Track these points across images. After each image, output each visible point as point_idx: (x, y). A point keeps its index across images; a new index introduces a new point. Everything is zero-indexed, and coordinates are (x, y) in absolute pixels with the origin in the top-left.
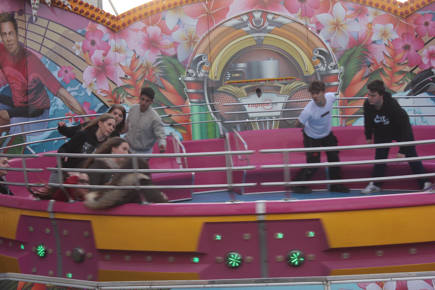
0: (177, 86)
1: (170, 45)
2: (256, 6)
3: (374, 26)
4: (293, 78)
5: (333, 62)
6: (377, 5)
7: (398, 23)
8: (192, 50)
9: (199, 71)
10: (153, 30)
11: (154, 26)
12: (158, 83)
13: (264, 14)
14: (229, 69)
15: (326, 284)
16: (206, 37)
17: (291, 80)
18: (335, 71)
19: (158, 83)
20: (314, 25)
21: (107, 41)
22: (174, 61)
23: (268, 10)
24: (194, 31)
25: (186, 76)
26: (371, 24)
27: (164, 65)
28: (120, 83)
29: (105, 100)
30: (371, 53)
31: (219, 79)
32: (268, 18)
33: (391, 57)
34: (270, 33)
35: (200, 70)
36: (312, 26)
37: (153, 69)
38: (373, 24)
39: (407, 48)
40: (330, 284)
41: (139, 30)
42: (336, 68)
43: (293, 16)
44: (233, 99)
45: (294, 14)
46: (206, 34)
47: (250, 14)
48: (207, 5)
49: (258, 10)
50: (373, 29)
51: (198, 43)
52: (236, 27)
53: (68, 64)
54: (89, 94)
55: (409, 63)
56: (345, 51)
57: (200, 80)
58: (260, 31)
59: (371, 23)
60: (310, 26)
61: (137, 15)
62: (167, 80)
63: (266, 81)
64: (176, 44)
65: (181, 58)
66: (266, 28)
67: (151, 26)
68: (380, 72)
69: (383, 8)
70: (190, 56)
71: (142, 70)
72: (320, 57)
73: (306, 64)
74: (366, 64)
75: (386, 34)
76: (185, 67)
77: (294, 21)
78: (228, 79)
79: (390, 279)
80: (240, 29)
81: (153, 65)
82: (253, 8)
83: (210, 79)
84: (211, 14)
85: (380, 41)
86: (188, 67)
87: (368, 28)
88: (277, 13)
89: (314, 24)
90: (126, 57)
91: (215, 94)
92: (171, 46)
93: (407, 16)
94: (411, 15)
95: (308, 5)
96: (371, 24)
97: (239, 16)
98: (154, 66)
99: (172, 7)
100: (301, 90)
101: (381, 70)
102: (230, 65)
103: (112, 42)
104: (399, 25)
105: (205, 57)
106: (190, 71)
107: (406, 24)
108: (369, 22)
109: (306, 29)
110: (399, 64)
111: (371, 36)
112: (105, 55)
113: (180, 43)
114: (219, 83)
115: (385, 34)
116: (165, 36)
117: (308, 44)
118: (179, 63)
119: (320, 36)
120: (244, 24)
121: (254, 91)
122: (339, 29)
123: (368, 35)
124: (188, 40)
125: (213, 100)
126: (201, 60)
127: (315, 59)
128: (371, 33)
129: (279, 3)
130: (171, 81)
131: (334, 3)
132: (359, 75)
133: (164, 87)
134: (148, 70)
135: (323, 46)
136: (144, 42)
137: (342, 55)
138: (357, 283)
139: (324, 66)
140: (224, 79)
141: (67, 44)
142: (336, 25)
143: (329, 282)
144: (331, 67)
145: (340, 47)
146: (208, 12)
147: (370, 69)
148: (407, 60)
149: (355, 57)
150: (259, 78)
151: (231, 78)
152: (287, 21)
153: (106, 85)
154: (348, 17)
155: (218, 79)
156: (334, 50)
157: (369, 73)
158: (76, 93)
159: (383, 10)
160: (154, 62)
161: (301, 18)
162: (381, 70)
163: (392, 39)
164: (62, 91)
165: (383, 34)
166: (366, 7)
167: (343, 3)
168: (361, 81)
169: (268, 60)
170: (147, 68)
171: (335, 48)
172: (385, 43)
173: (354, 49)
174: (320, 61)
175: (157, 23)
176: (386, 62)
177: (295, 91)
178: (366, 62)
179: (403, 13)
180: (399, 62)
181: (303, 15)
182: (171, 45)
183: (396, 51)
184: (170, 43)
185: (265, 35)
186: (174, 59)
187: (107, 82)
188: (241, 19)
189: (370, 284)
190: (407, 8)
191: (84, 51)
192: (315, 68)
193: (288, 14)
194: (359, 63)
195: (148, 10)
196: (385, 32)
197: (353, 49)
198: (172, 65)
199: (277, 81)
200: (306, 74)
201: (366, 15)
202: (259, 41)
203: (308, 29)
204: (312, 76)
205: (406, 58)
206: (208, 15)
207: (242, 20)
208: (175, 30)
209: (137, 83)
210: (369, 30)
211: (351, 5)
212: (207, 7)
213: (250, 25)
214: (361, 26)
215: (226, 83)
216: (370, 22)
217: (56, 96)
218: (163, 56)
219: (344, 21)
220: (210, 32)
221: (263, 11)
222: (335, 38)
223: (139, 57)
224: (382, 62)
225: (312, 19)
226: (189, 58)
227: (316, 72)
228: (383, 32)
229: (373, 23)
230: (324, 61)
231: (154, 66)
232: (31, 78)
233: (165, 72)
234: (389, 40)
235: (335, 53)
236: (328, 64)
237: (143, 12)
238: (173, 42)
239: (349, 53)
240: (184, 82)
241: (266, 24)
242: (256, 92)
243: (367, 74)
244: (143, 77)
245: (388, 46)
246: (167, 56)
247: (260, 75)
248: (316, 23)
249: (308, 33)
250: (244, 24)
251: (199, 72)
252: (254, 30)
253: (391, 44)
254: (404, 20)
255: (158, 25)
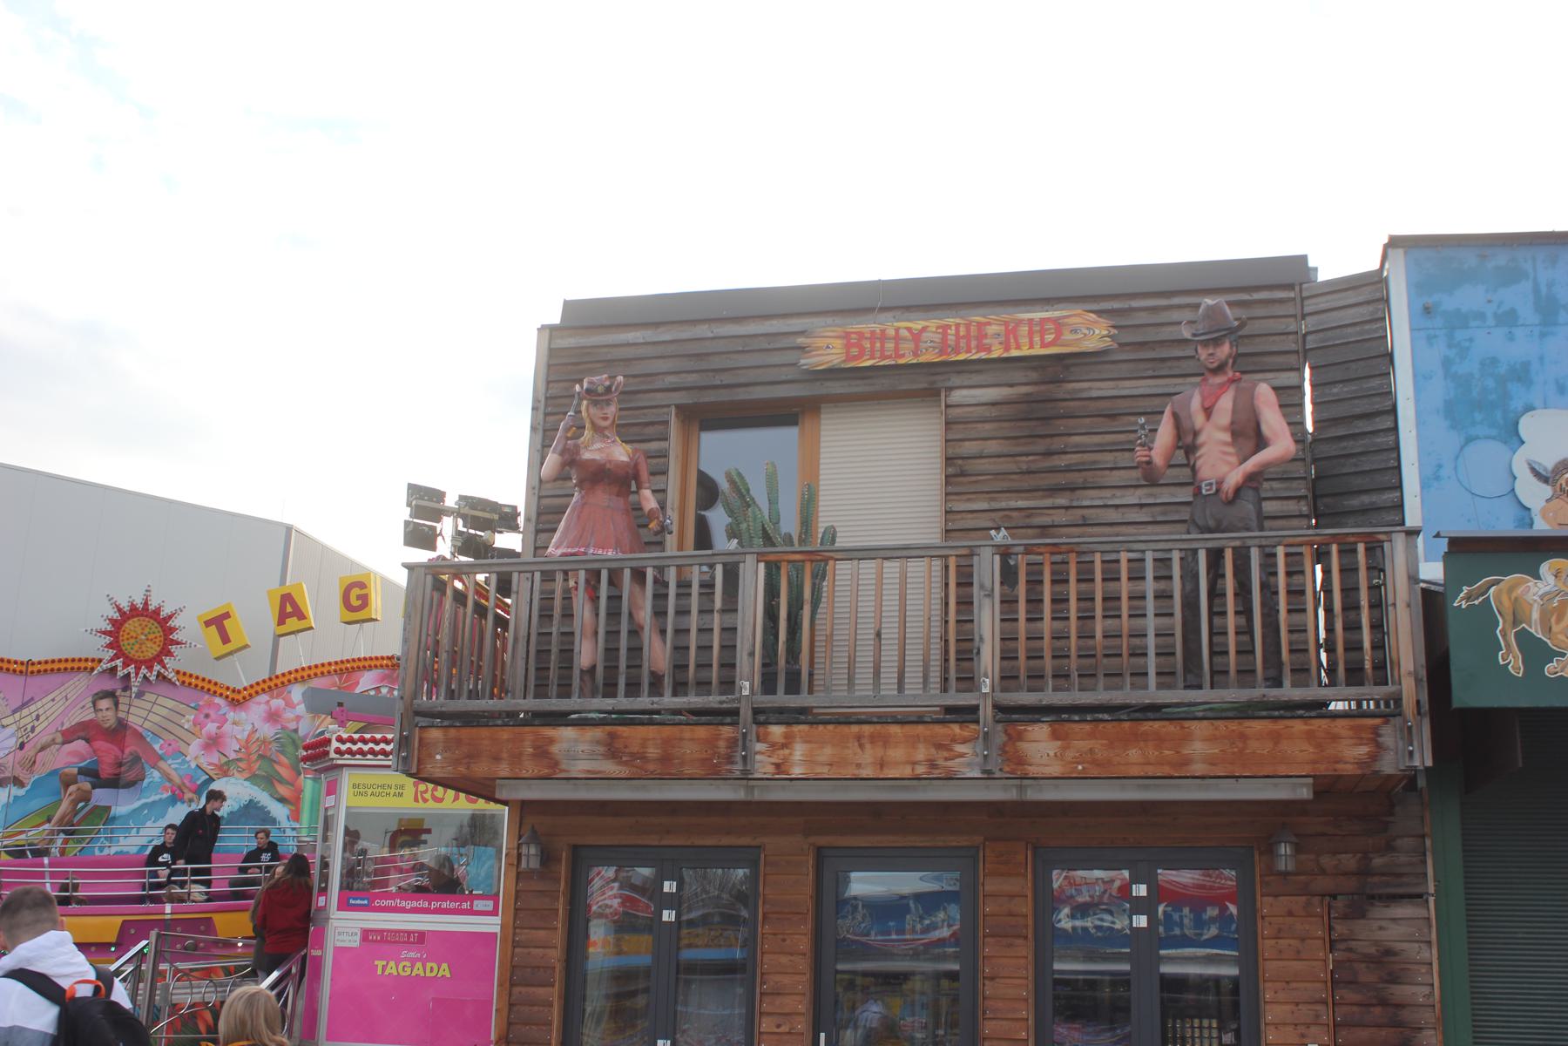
21: (225, 714)
22: (293, 735)
28: (233, 756)
29: (211, 773)
37: (270, 743)
47: (377, 689)
53: (172, 737)
54: (193, 765)
64: (298, 718)
65: (301, 733)
67: (275, 700)
90: (243, 730)
103: (231, 715)
112: (219, 728)
116: (288, 709)
118: (299, 737)
141: (176, 718)
153: (215, 758)
158: (177, 766)
164: (161, 764)
170: (264, 742)
187: (217, 755)
191: (195, 723)
208: (298, 704)
217: (153, 768)
232: (127, 751)
233: (282, 746)
255: (283, 699)
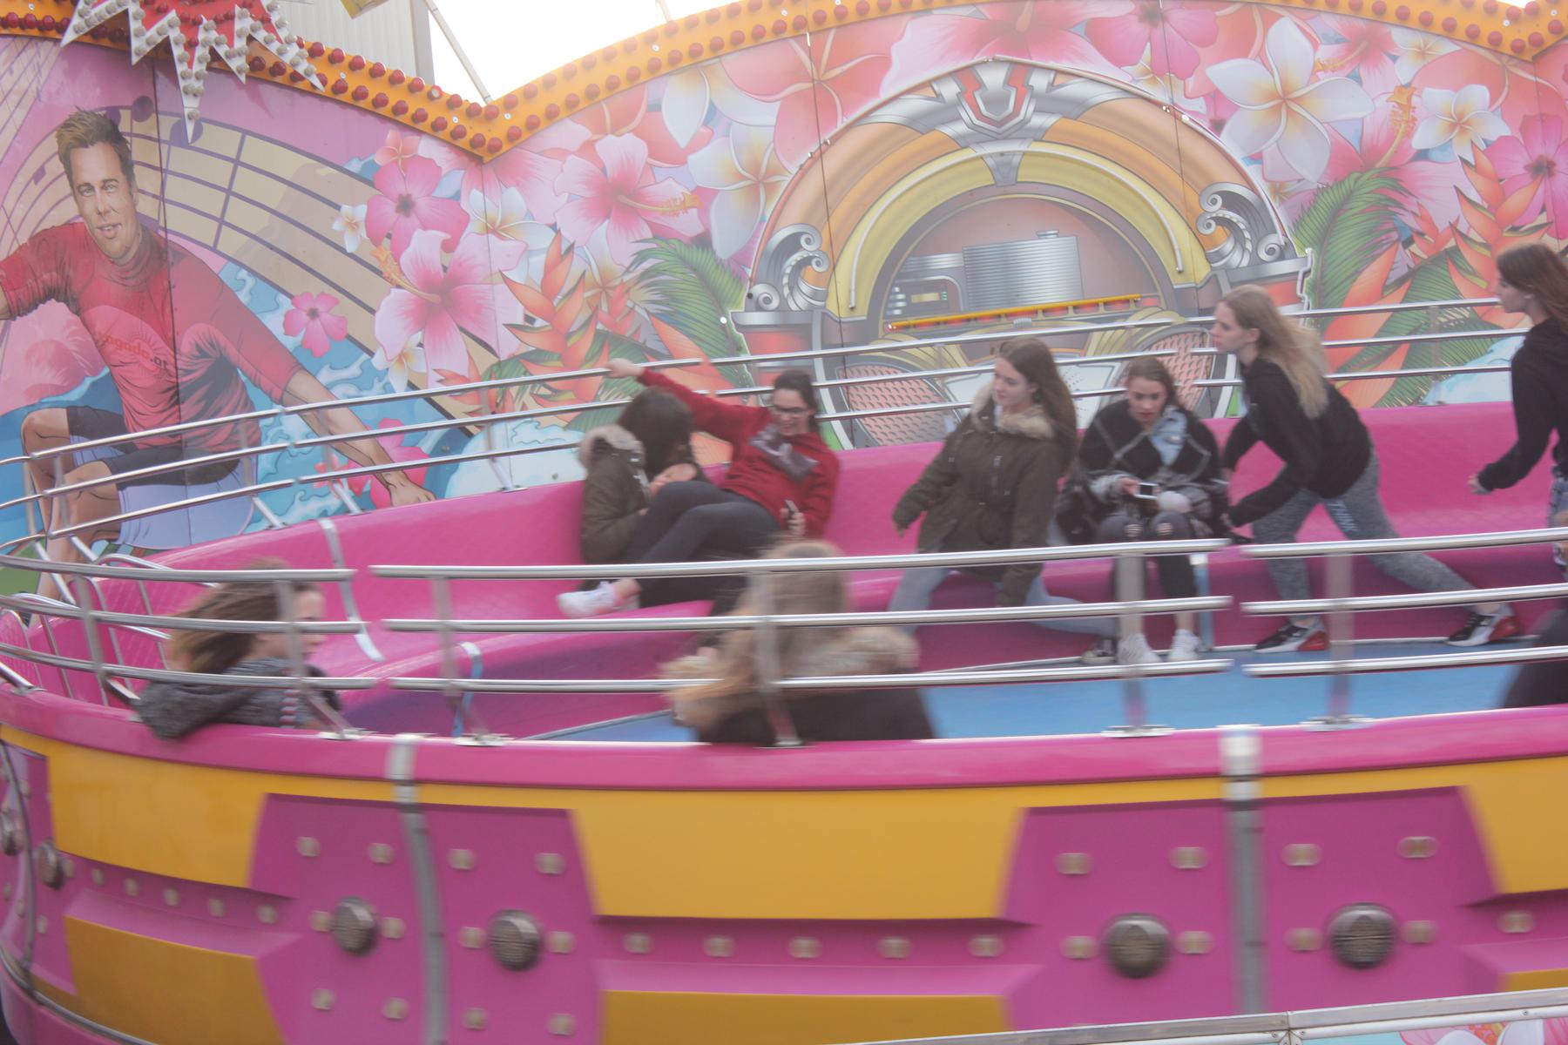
0: (713, 346)
1: (683, 199)
2: (988, 45)
3: (1420, 96)
4: (1133, 298)
5: (1275, 232)
6: (1426, 21)
7: (1507, 83)
8: (763, 214)
9: (791, 289)
10: (621, 148)
11: (621, 135)
12: (645, 341)
13: (1019, 73)
14: (900, 276)
15: (1286, 1039)
16: (811, 166)
17: (1126, 305)
18: (1286, 267)
19: (645, 341)
20: (1199, 105)
21: (457, 196)
22: (698, 257)
23: (1030, 58)
24: (766, 150)
25: (746, 311)
26: (1407, 89)
27: (664, 274)
28: (509, 345)
30: (1416, 197)
31: (866, 314)
32: (1032, 87)
33: (1486, 206)
34: (1041, 141)
35: (793, 286)
36: (1195, 108)
37: (626, 290)
38: (1415, 89)
39: (1542, 169)
40: (1302, 1039)
41: (566, 153)
42: (1287, 254)
43: (1122, 75)
44: (919, 384)
45: (1127, 68)
46: (811, 153)
47: (966, 76)
48: (810, 51)
49: (993, 59)
50: (1414, 108)
51: (784, 188)
52: (917, 124)
53: (317, 287)
55: (1553, 226)
56: (1318, 192)
57: (795, 320)
58: (1008, 133)
59: (1408, 85)
60: (1187, 108)
61: (558, 97)
62: (675, 325)
63: (1034, 312)
64: (702, 197)
65: (724, 244)
66: (1025, 121)
67: (611, 137)
68: (1449, 263)
69: (1449, 28)
70: (755, 235)
71: (587, 294)
72: (1228, 217)
73: (1176, 247)
74: (1395, 236)
75: (1465, 123)
76: (739, 278)
77: (1126, 91)
78: (897, 312)
79: (1519, 1013)
80: (932, 129)
81: (623, 274)
82: (975, 55)
83: (832, 318)
84: (824, 81)
85: (1442, 148)
86: (750, 275)
87: (1396, 105)
88: (1064, 65)
89: (1202, 98)
90: (527, 252)
91: (854, 369)
92: (688, 204)
93: (1536, 53)
94: (1553, 48)
95: (1176, 30)
96: (1406, 90)
97: (928, 84)
98: (627, 278)
99: (683, 64)
100: (1163, 339)
101: (1452, 256)
102: (902, 261)
103: (474, 201)
104: (1509, 87)
105: (810, 237)
106: (760, 290)
107: (1537, 83)
108: (1399, 84)
109: (1172, 120)
110: (1515, 229)
111: (1409, 134)
112: (449, 247)
113: (719, 190)
114: (866, 331)
115: (1459, 123)
117: (1181, 175)
118: (719, 264)
119: (1224, 140)
120: (948, 113)
121: (992, 353)
122: (1290, 112)
123: (1398, 131)
124: (749, 179)
125: (845, 391)
126: (798, 248)
127: (1209, 226)
128: (1407, 122)
129: (1072, 30)
130: (694, 329)
131: (1270, 20)
132: (1370, 275)
133: (666, 352)
134: (606, 293)
135: (1238, 178)
136: (588, 194)
137: (1306, 209)
138: (1400, 1031)
139: (1244, 249)
140: (885, 313)
142: (1280, 101)
143: (1297, 1032)
144: (1270, 252)
145: (1300, 178)
146: (816, 77)
147: (1412, 253)
148: (1545, 213)
149: (1355, 211)
150: (1011, 304)
151: (910, 310)
152: (1100, 94)
153: (456, 356)
154: (1324, 69)
155: (861, 315)
156: (1278, 190)
157: (1408, 266)
159: (1451, 39)
160: (627, 265)
161: (1153, 81)
162: (1452, 256)
163: (1485, 141)
164: (300, 384)
165: (1453, 123)
166: (1387, 29)
167: (1304, 20)
168: (1383, 297)
169: (1039, 237)
170: (604, 286)
171: (1282, 184)
172: (1463, 157)
173: (1349, 184)
174: (1227, 230)
175: (633, 126)
176: (1468, 225)
177: (1143, 343)
178: (1395, 229)
179: (1524, 46)
180: (1516, 225)
181: (1157, 71)
182: (684, 201)
183: (1501, 183)
184: (683, 193)
185: (1024, 147)
186: (700, 250)
188: (934, 96)
189: (1447, 1032)
190: (1538, 25)
191: (376, 233)
192: (1210, 259)
193: (1104, 68)
194: (1370, 233)
195: (599, 78)
196: (1460, 116)
197: (1347, 184)
198: (694, 270)
199: (1075, 312)
200: (1178, 283)
201: (1387, 59)
202: (1005, 173)
203: (1180, 120)
204: (1201, 287)
205: (1541, 206)
206: (814, 85)
207: (938, 96)
208: (696, 145)
209: (572, 341)
210: (1400, 112)
211: (1330, 24)
212: (810, 57)
213: (967, 114)
214: (1373, 100)
215: (890, 327)
216: (1404, 83)
217: (281, 402)
218: (659, 242)
219: (1307, 85)
220: (824, 147)
221: (1012, 62)
222: (1278, 146)
223: (571, 248)
224: (1453, 227)
225: (1191, 81)
226: (751, 242)
227: (1214, 272)
228: (1454, 116)
229: (1415, 85)
230: (1241, 230)
231: (627, 278)
232: (186, 344)
233: (670, 297)
234: (1477, 143)
235: (1282, 201)
236: (1257, 242)
237: (578, 88)
238: (692, 187)
239: (1338, 198)
240: (739, 331)
241: (1028, 108)
242: (998, 354)
243: (1401, 271)
244: (587, 323)
245: (1475, 167)
246: (673, 241)
247: (1012, 292)
248: (1205, 96)
249: (1179, 134)
250: (948, 113)
251: (791, 293)
252: (986, 132)
253: (1485, 162)
254: (1524, 70)
255: (637, 132)
